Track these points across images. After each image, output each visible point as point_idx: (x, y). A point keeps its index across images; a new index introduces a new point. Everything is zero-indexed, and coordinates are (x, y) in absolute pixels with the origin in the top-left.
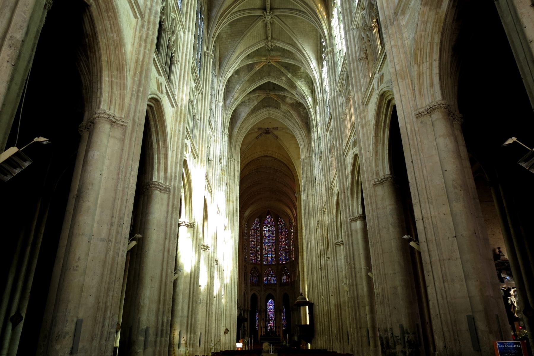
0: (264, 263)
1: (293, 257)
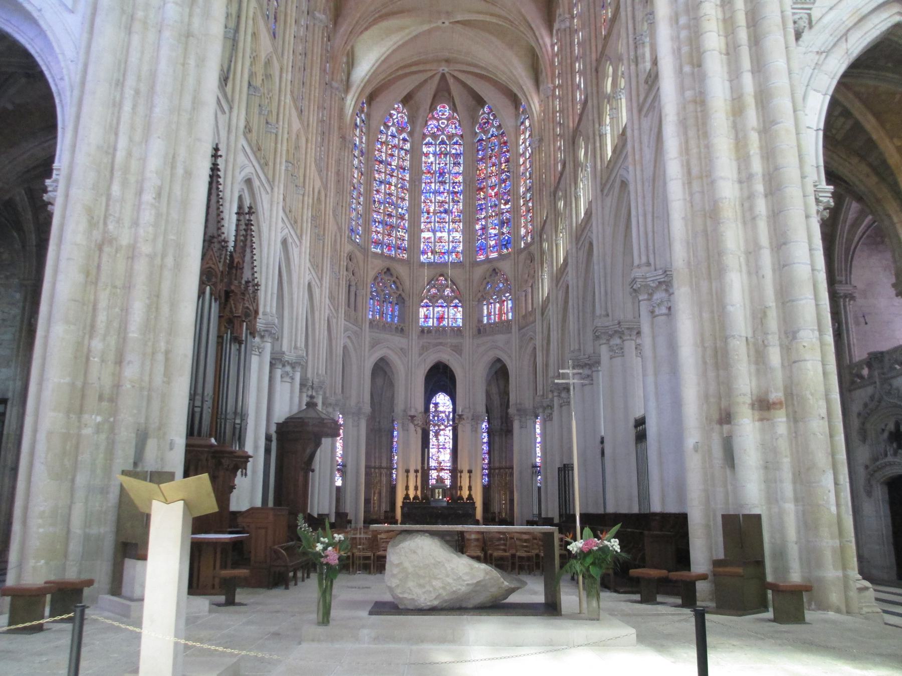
0: (423, 258)
1: (527, 233)
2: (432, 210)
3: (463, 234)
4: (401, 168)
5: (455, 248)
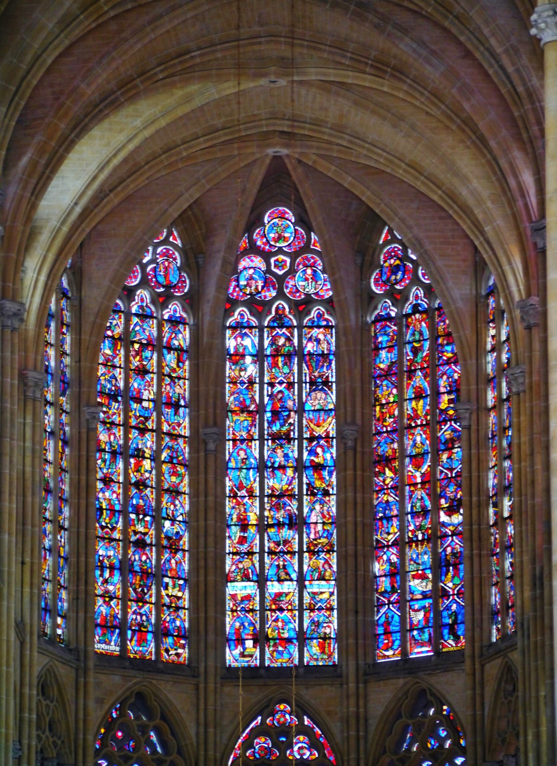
1: (506, 606)
2: (253, 519)
3: (338, 586)
4: (169, 404)
5: (318, 624)
